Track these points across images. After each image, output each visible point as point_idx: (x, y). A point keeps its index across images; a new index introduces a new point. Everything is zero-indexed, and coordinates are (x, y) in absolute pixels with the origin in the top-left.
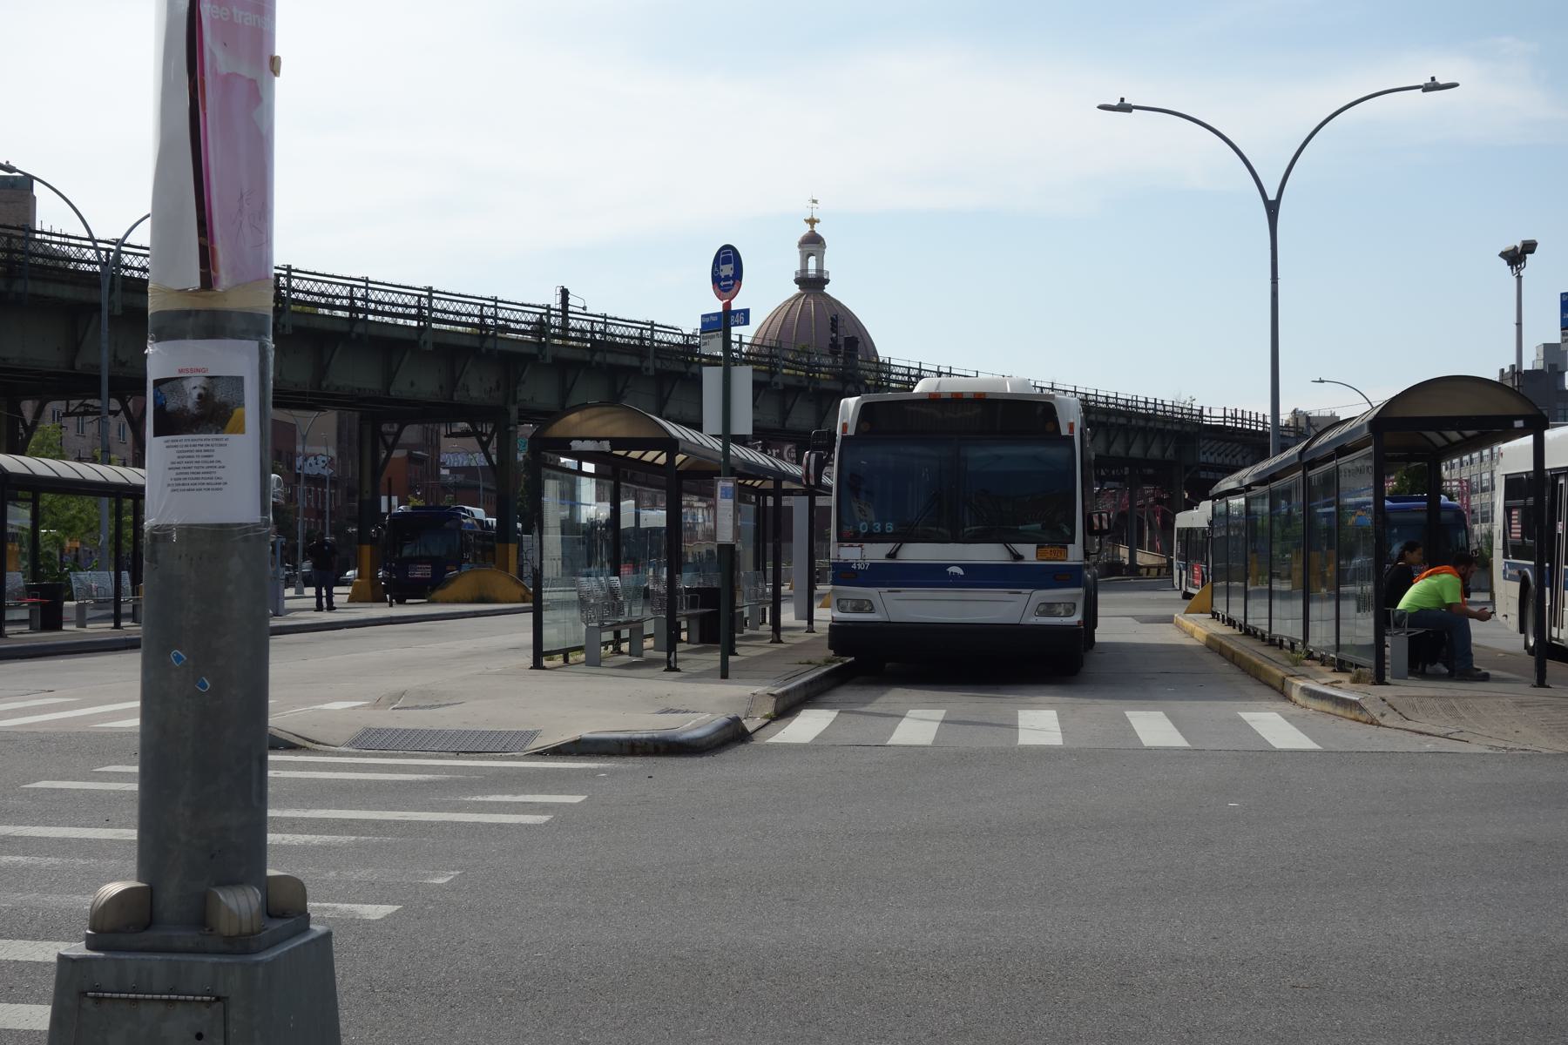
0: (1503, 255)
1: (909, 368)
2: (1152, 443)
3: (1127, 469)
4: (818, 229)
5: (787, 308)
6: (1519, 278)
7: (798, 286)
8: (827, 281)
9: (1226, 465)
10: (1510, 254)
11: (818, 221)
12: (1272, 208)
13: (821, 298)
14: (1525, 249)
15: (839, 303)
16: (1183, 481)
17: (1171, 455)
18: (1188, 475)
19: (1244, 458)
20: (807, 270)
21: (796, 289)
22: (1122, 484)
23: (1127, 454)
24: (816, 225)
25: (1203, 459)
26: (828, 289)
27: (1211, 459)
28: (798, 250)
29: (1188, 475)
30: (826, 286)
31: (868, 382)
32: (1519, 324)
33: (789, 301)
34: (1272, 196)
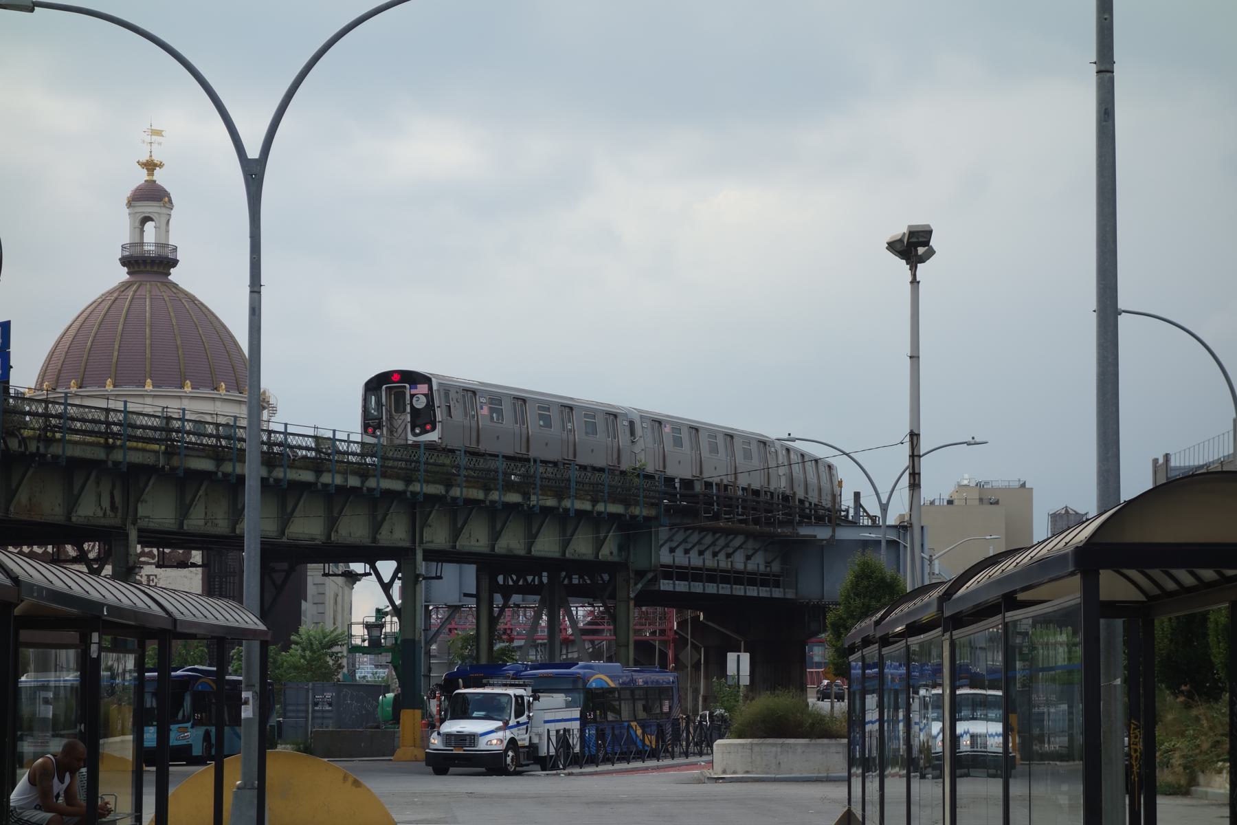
0: (893, 246)
1: (108, 410)
2: (572, 535)
3: (545, 574)
4: (160, 177)
5: (107, 304)
6: (915, 282)
7: (125, 269)
8: (174, 263)
9: (737, 572)
10: (898, 247)
11: (161, 165)
12: (254, 172)
13: (163, 288)
14: (914, 240)
15: (192, 299)
16: (632, 595)
17: (611, 553)
18: (639, 586)
19: (748, 558)
20: (142, 244)
21: (122, 274)
22: (538, 598)
23: (529, 551)
24: (157, 171)
25: (665, 557)
26: (175, 275)
27: (680, 559)
28: (127, 211)
29: (639, 586)
30: (172, 270)
31: (26, 433)
32: (915, 358)
33: (110, 293)
34: (253, 152)
